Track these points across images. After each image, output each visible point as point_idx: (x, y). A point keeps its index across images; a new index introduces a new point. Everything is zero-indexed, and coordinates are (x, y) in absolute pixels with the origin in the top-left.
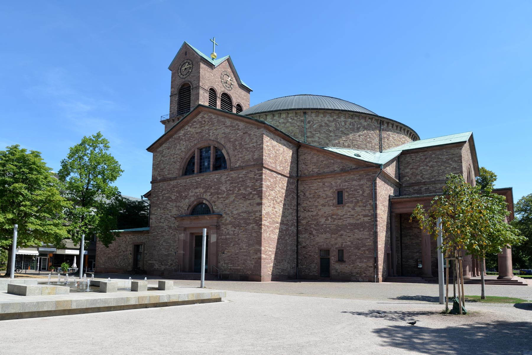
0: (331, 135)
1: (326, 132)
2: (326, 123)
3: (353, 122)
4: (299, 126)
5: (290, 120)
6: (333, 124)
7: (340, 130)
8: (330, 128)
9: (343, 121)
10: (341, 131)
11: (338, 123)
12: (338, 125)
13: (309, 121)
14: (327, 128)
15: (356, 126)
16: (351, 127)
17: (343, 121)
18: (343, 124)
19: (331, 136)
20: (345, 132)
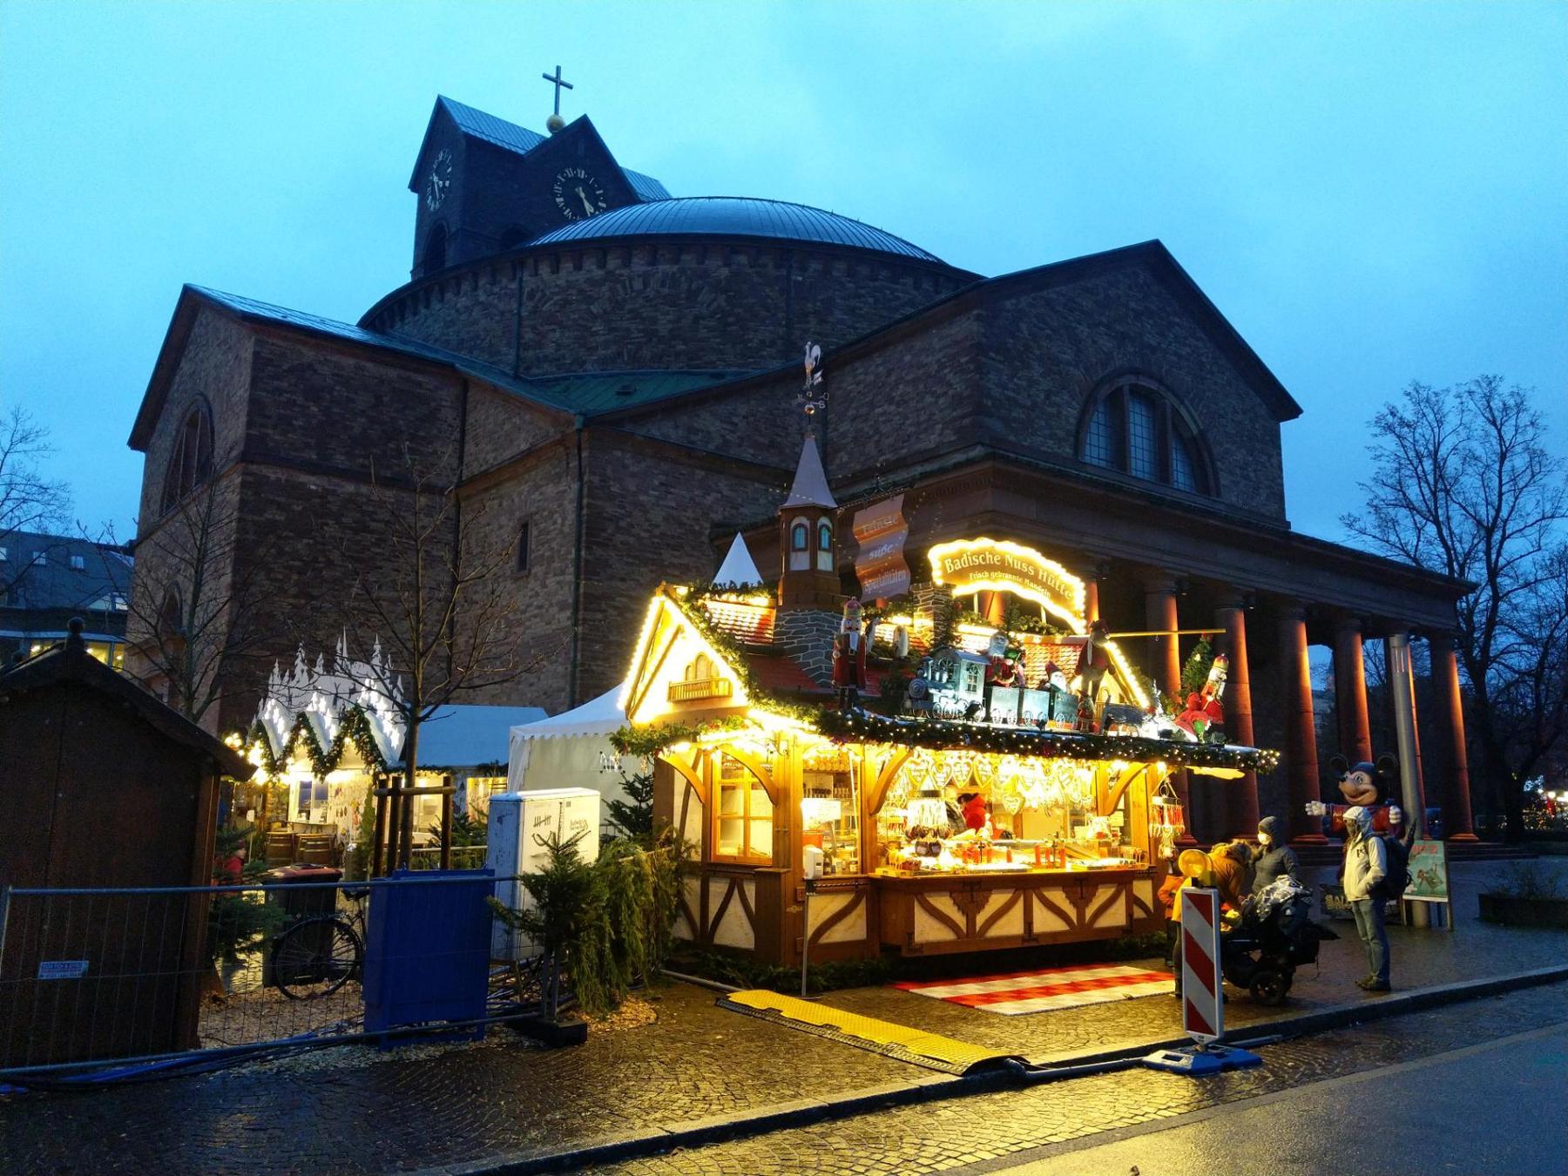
0: (594, 329)
1: (580, 322)
2: (581, 291)
3: (674, 274)
4: (502, 313)
5: (482, 298)
6: (604, 289)
7: (628, 307)
8: (592, 307)
9: (639, 276)
10: (630, 311)
11: (619, 286)
12: (621, 291)
13: (532, 290)
14: (584, 307)
15: (684, 286)
16: (666, 291)
17: (639, 276)
18: (638, 285)
19: (596, 333)
20: (645, 315)
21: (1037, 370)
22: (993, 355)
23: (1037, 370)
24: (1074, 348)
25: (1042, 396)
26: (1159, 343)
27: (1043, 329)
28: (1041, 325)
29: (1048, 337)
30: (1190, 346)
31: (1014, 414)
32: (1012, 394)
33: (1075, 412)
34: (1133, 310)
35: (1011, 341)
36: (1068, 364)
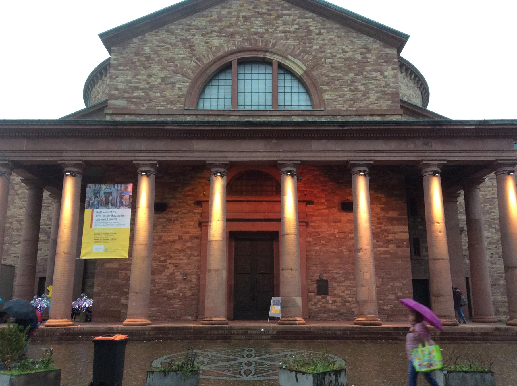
21: (156, 67)
22: (122, 68)
23: (156, 67)
24: (189, 50)
25: (159, 80)
26: (267, 30)
27: (163, 46)
28: (162, 44)
29: (168, 49)
30: (297, 24)
31: (135, 94)
32: (134, 85)
33: (188, 84)
34: (243, 17)
35: (136, 57)
36: (184, 59)
